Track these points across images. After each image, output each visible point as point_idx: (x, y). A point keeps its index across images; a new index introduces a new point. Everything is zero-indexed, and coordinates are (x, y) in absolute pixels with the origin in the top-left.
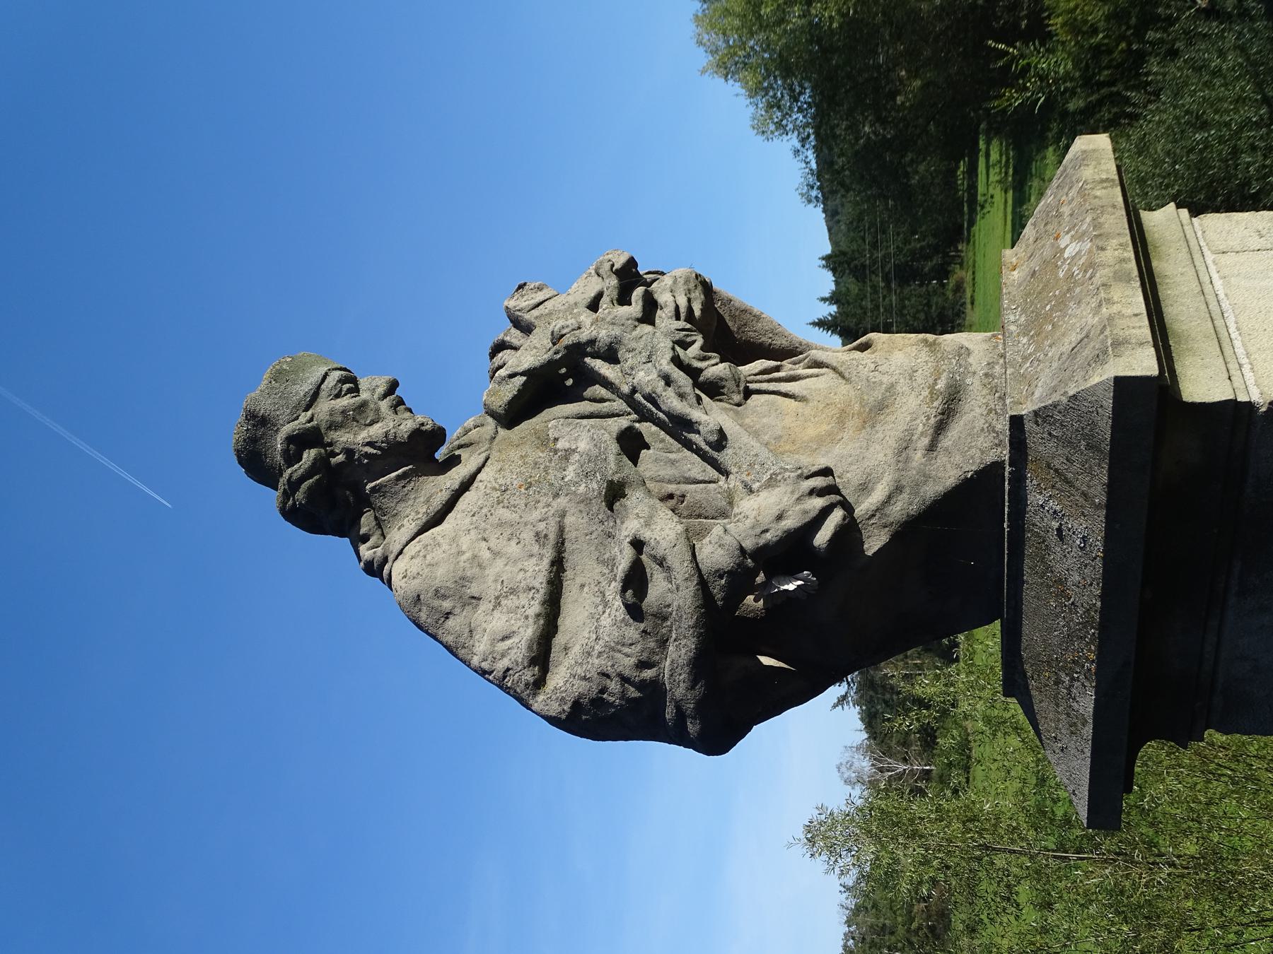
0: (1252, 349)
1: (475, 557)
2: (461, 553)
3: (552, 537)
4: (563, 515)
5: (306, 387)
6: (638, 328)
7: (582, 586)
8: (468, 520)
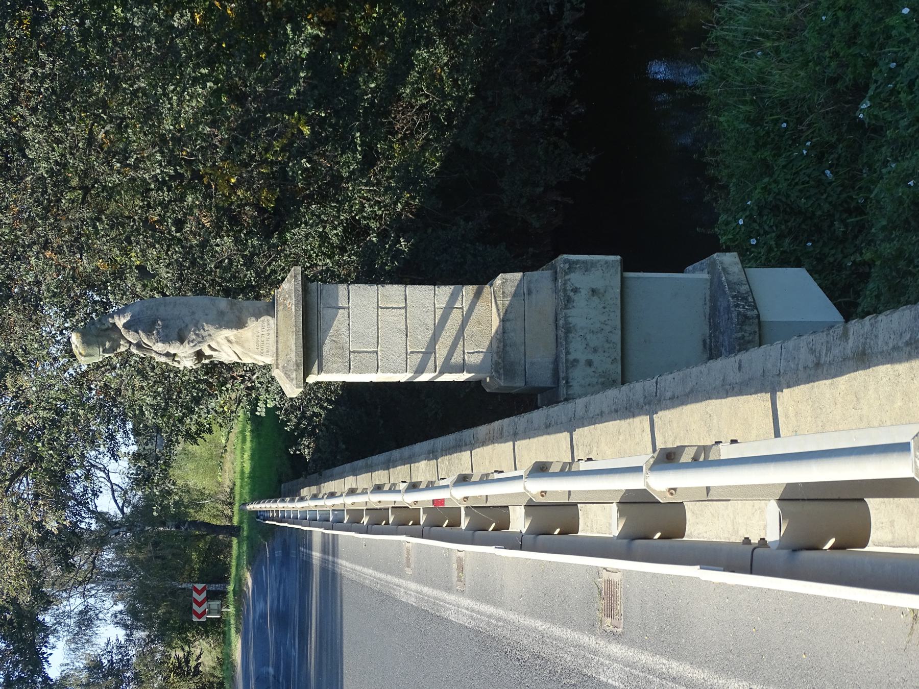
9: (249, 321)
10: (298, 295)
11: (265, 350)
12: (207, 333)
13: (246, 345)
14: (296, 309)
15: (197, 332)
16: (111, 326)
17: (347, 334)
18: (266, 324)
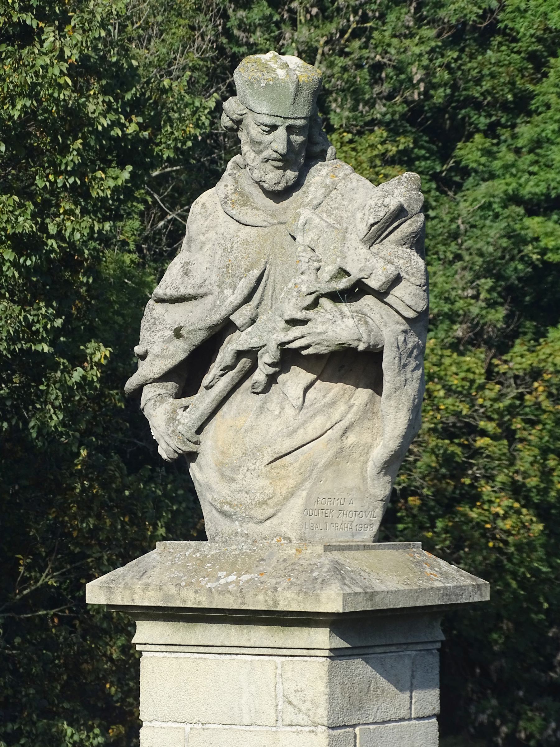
0: (181, 661)
1: (204, 243)
2: (204, 234)
3: (202, 291)
4: (211, 294)
5: (253, 104)
6: (280, 319)
7: (192, 312)
8: (222, 231)
9: (388, 478)
10: (456, 595)
11: (314, 518)
12: (409, 375)
13: (329, 474)
14: (438, 589)
15: (415, 353)
16: (317, 149)
17: (379, 719)
18: (365, 520)
